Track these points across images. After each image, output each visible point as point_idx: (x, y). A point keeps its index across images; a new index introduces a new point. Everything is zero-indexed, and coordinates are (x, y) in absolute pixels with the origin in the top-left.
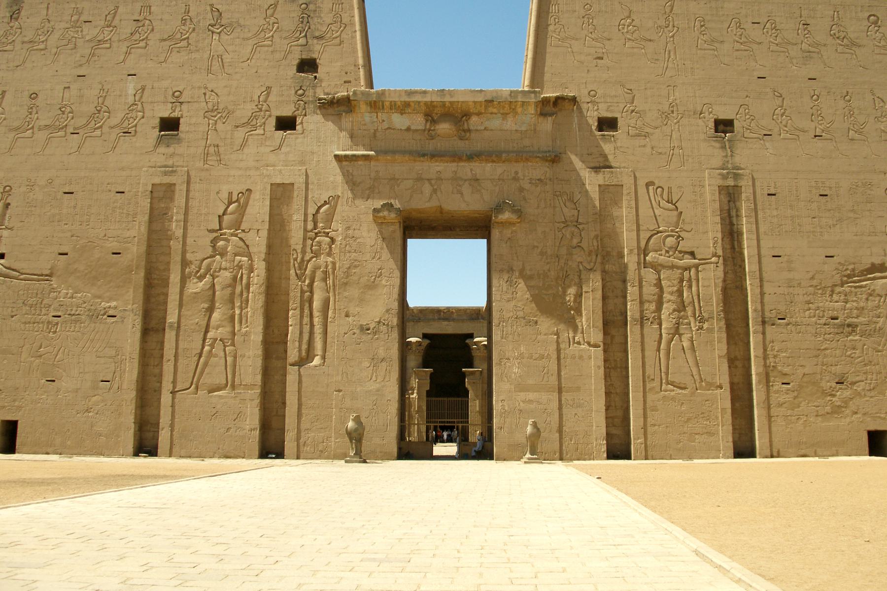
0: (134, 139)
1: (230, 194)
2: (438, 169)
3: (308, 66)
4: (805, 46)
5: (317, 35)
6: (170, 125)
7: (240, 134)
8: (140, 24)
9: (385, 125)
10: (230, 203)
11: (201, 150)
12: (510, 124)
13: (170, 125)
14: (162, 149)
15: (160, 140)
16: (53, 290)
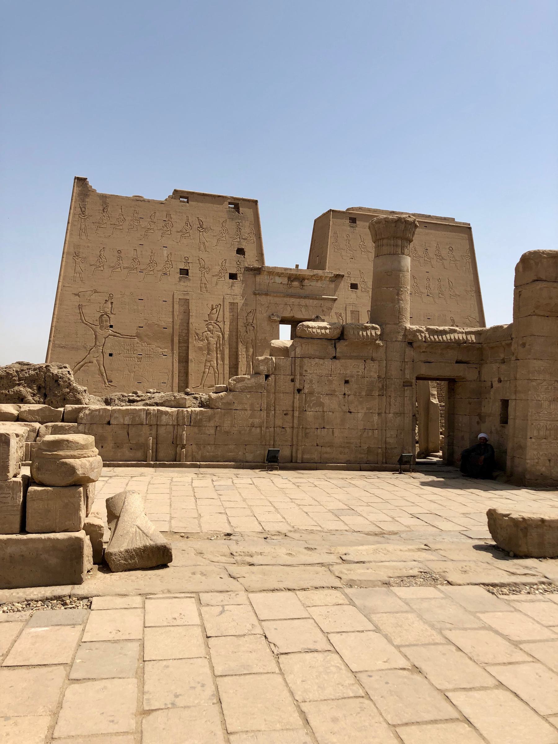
0: (169, 278)
1: (212, 305)
2: (293, 301)
3: (240, 251)
4: (426, 258)
5: (244, 237)
6: (185, 272)
7: (215, 279)
8: (167, 222)
9: (273, 281)
10: (213, 309)
11: (199, 286)
12: (319, 284)
13: (185, 272)
14: (182, 283)
15: (180, 279)
16: (138, 343)
